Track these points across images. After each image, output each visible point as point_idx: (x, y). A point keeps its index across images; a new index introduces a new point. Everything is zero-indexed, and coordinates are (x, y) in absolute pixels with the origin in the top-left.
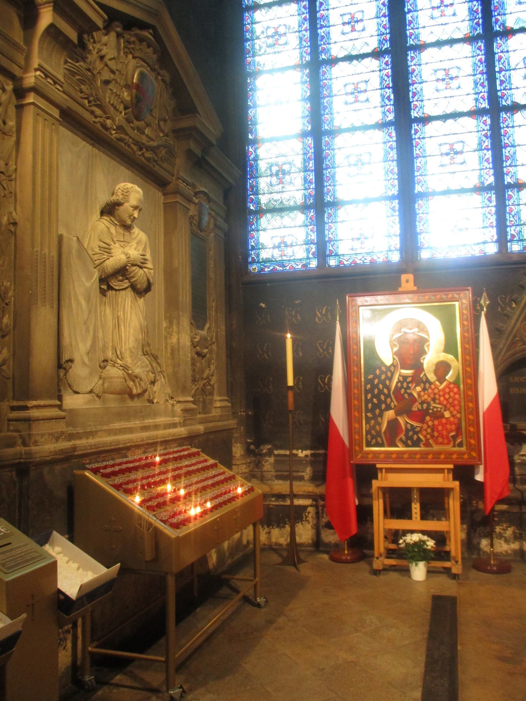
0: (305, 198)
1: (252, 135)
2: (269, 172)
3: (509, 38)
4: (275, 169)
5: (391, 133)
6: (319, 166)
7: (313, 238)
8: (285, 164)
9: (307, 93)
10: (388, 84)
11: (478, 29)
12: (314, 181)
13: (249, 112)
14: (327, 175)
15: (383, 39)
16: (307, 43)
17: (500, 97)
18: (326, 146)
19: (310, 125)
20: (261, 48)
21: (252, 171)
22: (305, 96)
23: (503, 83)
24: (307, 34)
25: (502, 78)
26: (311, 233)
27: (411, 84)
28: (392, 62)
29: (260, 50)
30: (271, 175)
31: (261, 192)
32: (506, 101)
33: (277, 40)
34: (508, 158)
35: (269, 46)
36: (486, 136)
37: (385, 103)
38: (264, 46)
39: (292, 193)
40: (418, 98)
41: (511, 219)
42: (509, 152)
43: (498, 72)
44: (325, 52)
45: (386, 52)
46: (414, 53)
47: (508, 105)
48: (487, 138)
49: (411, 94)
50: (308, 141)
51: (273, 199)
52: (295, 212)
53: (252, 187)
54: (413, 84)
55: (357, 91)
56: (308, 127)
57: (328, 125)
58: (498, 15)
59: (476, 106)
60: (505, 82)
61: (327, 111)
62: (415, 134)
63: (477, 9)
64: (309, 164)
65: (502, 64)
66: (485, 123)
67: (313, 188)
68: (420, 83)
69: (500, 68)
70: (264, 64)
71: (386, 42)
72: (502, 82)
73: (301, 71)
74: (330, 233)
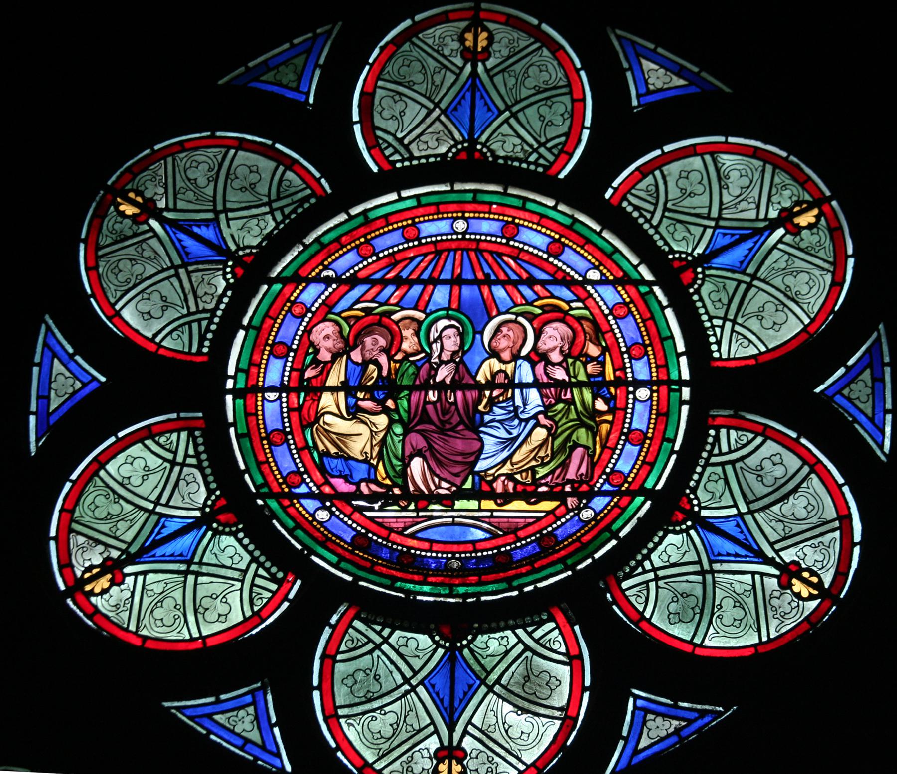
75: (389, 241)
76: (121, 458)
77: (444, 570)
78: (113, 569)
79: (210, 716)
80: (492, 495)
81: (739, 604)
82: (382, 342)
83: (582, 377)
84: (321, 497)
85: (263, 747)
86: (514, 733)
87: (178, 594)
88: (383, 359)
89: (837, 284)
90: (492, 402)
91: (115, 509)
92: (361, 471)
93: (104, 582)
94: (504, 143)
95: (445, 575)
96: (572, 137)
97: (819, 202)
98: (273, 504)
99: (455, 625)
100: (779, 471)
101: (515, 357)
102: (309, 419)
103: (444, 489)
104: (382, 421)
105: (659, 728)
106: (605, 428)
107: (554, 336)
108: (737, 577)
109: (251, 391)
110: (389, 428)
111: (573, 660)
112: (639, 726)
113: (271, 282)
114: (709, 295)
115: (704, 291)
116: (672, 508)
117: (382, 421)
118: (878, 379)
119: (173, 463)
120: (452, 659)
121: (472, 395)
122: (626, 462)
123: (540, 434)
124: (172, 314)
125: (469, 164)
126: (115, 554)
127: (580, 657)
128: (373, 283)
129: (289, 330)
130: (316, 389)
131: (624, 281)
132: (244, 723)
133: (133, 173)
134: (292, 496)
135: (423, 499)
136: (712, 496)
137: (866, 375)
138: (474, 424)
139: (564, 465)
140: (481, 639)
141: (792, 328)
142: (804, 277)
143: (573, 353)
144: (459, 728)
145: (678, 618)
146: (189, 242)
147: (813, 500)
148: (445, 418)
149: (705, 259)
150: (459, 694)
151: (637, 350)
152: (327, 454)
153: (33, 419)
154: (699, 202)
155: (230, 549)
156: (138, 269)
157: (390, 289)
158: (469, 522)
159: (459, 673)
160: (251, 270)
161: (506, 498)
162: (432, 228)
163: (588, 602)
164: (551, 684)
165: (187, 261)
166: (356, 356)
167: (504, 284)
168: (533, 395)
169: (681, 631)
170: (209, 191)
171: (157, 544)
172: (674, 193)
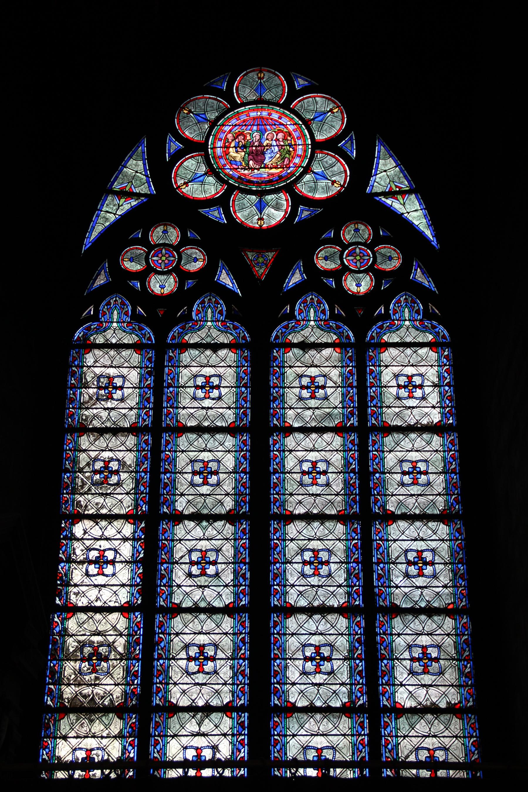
0: (126, 697)
1: (60, 600)
2: (79, 654)
3: (390, 523)
4: (87, 650)
5: (243, 622)
6: (148, 652)
7: (132, 755)
8: (102, 645)
9: (140, 553)
10: (243, 558)
11: (355, 507)
13: (60, 567)
14: (159, 668)
15: (242, 500)
16: (145, 489)
17: (377, 595)
18: (159, 628)
20: (84, 484)
21: (56, 650)
22: (137, 558)
24: (147, 477)
26: (130, 748)
29: (82, 487)
30: (83, 660)
31: (66, 681)
32: (383, 601)
33: (106, 478)
34: (384, 674)
36: (359, 641)
37: (239, 582)
39: (108, 688)
40: (280, 582)
41: (387, 755)
42: (386, 665)
43: (375, 563)
44: (167, 504)
45: (244, 516)
46: (277, 524)
47: (386, 606)
48: (360, 645)
50: (137, 617)
51: (80, 693)
52: (111, 715)
53: (53, 672)
54: (276, 562)
55: (204, 562)
56: (138, 600)
57: (164, 601)
58: (378, 494)
59: (348, 602)
60: (383, 576)
61: (164, 581)
62: (275, 628)
63: (355, 482)
64: (135, 649)
66: (358, 624)
67: (137, 684)
68: (283, 563)
70: (86, 506)
72: (380, 577)
74: (156, 750)
75: (243, 117)
76: (187, 161)
77: (257, 182)
78: (186, 184)
79: (208, 212)
80: (268, 168)
81: (323, 188)
82: (243, 138)
83: (287, 144)
84: (231, 169)
85: (220, 218)
86: (275, 215)
87: (200, 189)
88: (243, 141)
89: (343, 123)
90: (267, 149)
91: (186, 172)
92: (239, 164)
93: (184, 186)
94: (267, 96)
95: (258, 184)
96: (283, 95)
97: (338, 107)
98: (220, 171)
99: (261, 194)
100: (331, 162)
101: (272, 140)
102: (227, 153)
103: (257, 167)
104: (243, 153)
105: (306, 213)
106: (292, 154)
108: (322, 183)
109: (214, 148)
110: (245, 155)
111: (287, 200)
112: (302, 212)
113: (218, 126)
114: (314, 126)
115: (313, 126)
116: (307, 170)
117: (243, 153)
118: (352, 143)
119: (198, 163)
120: (260, 200)
121: (262, 148)
122: (297, 161)
123: (278, 155)
124: (196, 133)
125: (260, 101)
126: (186, 181)
127: (288, 200)
128: (240, 126)
129: (223, 136)
130: (228, 147)
131: (295, 124)
132: (216, 214)
133: (186, 104)
134: (224, 169)
135: (253, 169)
136: (317, 168)
137: (350, 142)
138: (263, 153)
139: (284, 162)
140: (267, 196)
141: (333, 133)
142: (335, 122)
143: (285, 139)
144: (263, 214)
145: (310, 192)
146: (199, 118)
147: (338, 168)
148: (257, 154)
149: (313, 119)
150: (262, 207)
151: (299, 138)
152: (231, 160)
153: (167, 154)
154: (312, 108)
155: (211, 179)
156: (188, 124)
157: (243, 127)
159: (262, 203)
160: (213, 124)
161: (271, 168)
162: (253, 114)
164: (282, 205)
165: (199, 122)
166: (237, 140)
167: (269, 125)
168: (276, 148)
169: (310, 194)
170: (203, 107)
171: (195, 179)
172: (306, 106)
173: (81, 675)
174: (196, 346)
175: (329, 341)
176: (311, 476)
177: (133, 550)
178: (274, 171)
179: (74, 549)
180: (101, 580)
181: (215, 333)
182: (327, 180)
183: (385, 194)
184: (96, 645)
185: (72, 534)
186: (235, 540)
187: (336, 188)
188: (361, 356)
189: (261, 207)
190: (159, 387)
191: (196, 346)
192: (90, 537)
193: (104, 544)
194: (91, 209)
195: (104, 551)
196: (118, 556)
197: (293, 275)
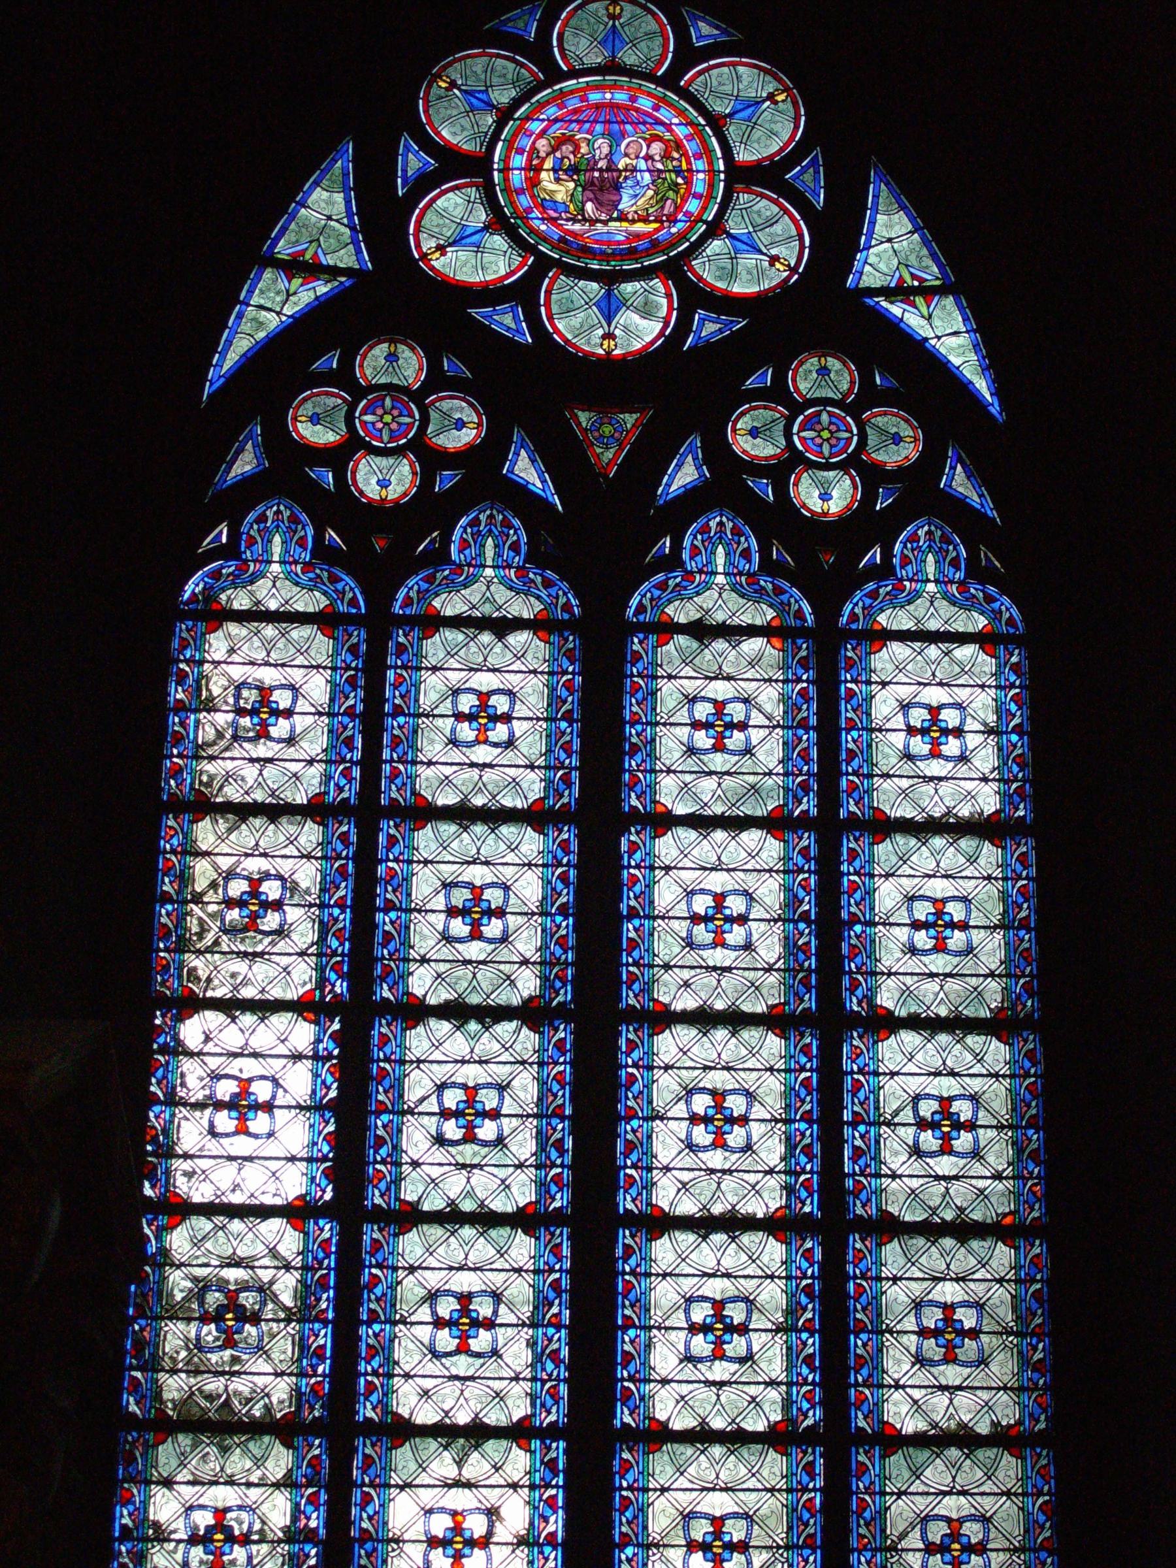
0: (299, 1400)
1: (153, 1187)
2: (195, 1306)
3: (882, 1036)
4: (214, 1299)
7: (313, 1524)
8: (247, 1288)
9: (329, 1088)
11: (807, 997)
12: (328, 1354)
13: (151, 1115)
15: (556, 975)
16: (342, 944)
17: (852, 1192)
19: (330, 1188)
21: (144, 1296)
23: (860, 1157)
24: (345, 919)
25: (858, 1142)
26: (310, 1509)
27: (624, 1118)
28: (575, 1044)
29: (201, 935)
30: (205, 1319)
31: (167, 1363)
33: (254, 917)
35: (230, 930)
36: (808, 1291)
37: (548, 1157)
38: (215, 926)
39: (260, 1381)
40: (639, 1160)
41: (861, 1531)
42: (865, 1345)
44: (390, 980)
45: (562, 1013)
46: (635, 1031)
47: (870, 1217)
48: (812, 1301)
49: (620, 1146)
50: (322, 1230)
52: (266, 1439)
53: (140, 1345)
54: (631, 1115)
55: (470, 1112)
56: (324, 1191)
57: (382, 1196)
59: (788, 1206)
60: (864, 1153)
61: (383, 1152)
63: (808, 943)
64: (318, 1300)
65: (861, 1104)
66: (808, 1255)
67: (324, 1375)
69: (854, 1112)
70: (209, 980)
71: (564, 985)
72: (858, 1153)
73: (316, 1022)
74: (365, 1515)
75: (573, 103)
78: (441, 249)
80: (627, 220)
81: (749, 273)
84: (543, 219)
89: (796, 127)
90: (626, 178)
93: (437, 255)
94: (629, 58)
95: (603, 257)
96: (663, 57)
97: (786, 89)
99: (610, 279)
101: (637, 157)
103: (604, 217)
104: (572, 185)
105: (710, 328)
107: (657, 148)
108: (749, 260)
109: (506, 170)
111: (669, 296)
114: (733, 131)
116: (716, 229)
118: (817, 172)
120: (609, 294)
122: (693, 206)
124: (466, 133)
125: (612, 67)
129: (526, 143)
130: (539, 169)
132: (508, 320)
133: (445, 68)
135: (593, 222)
136: (736, 225)
138: (617, 187)
139: (663, 208)
141: (775, 148)
143: (666, 156)
145: (720, 278)
146: (473, 101)
147: (785, 227)
148: (603, 186)
149: (731, 115)
150: (613, 307)
151: (698, 156)
154: (728, 88)
155: (498, 241)
157: (574, 125)
158: (618, 231)
160: (505, 115)
161: (633, 221)
162: (594, 97)
163: (675, 271)
164: (658, 306)
166: (558, 155)
167: (631, 123)
168: (647, 176)
169: (721, 285)
171: (463, 238)
172: (715, 83)
173: (200, 1350)
174: (457, 622)
175: (758, 622)
176: (711, 926)
177: (314, 1083)
178: (640, 227)
179: (183, 1075)
180: (241, 1145)
181: (501, 594)
182: (760, 253)
183: (888, 293)
184: (232, 1287)
185: (179, 1042)
186: (541, 1064)
187: (777, 275)
188: (826, 657)
189: (609, 309)
190: (372, 718)
191: (457, 622)
192: (218, 1050)
193: (250, 1067)
194: (224, 300)
195: (250, 1080)
196: (280, 1092)
197: (679, 466)
